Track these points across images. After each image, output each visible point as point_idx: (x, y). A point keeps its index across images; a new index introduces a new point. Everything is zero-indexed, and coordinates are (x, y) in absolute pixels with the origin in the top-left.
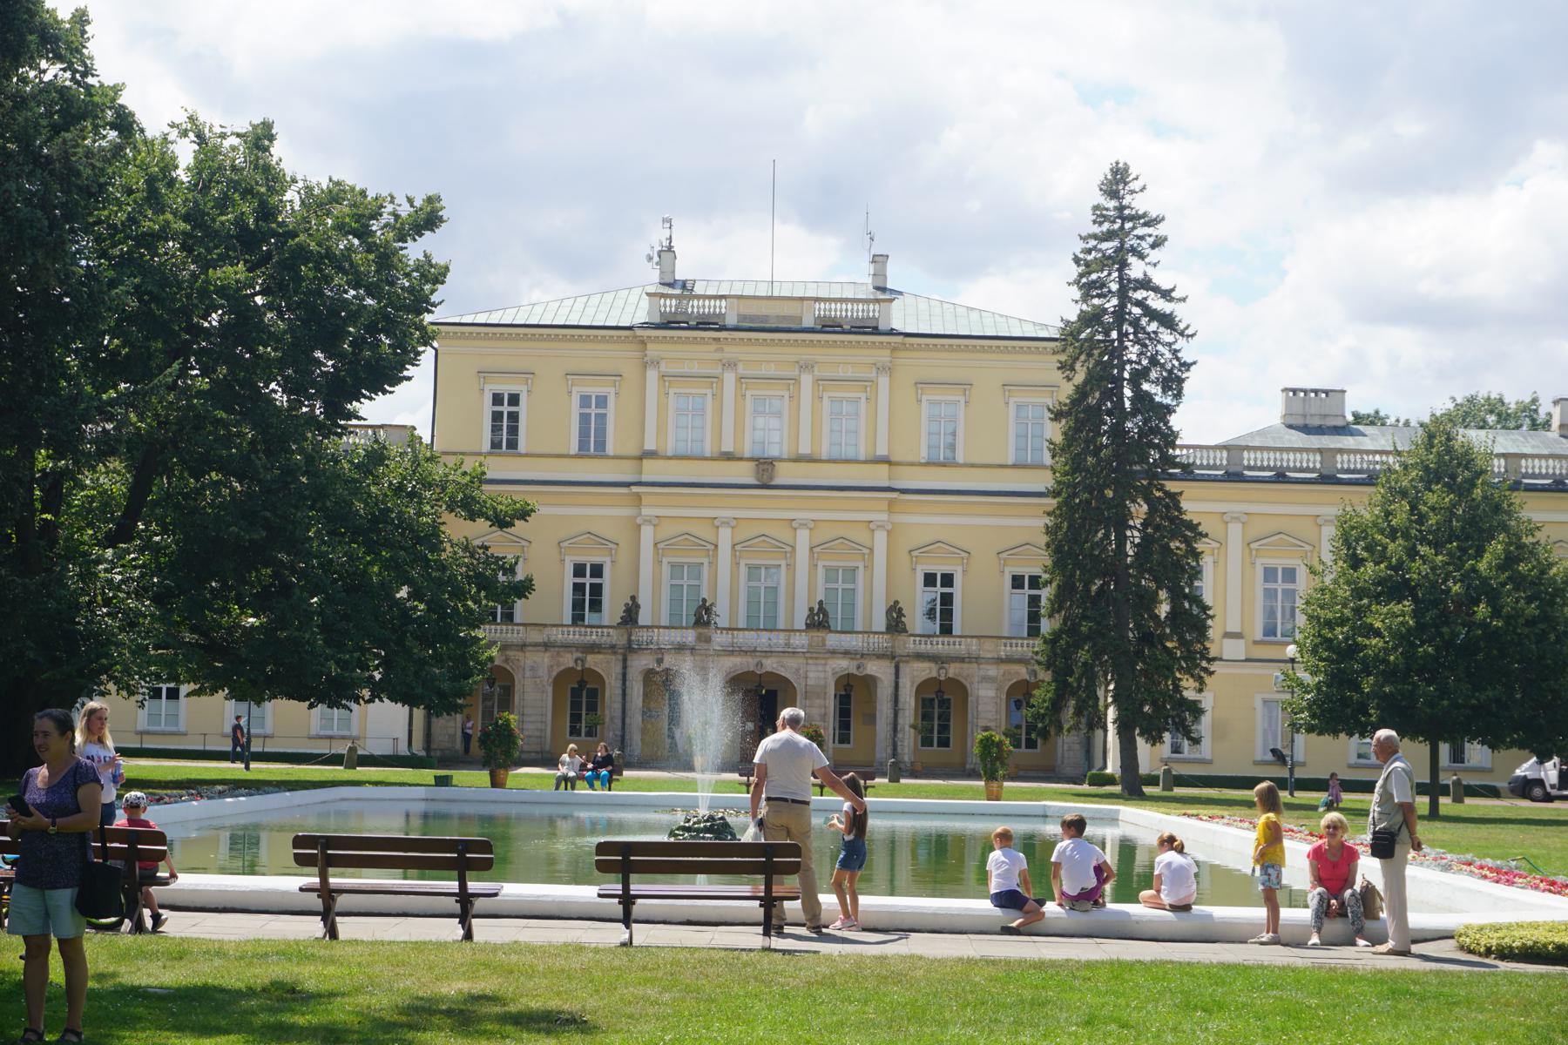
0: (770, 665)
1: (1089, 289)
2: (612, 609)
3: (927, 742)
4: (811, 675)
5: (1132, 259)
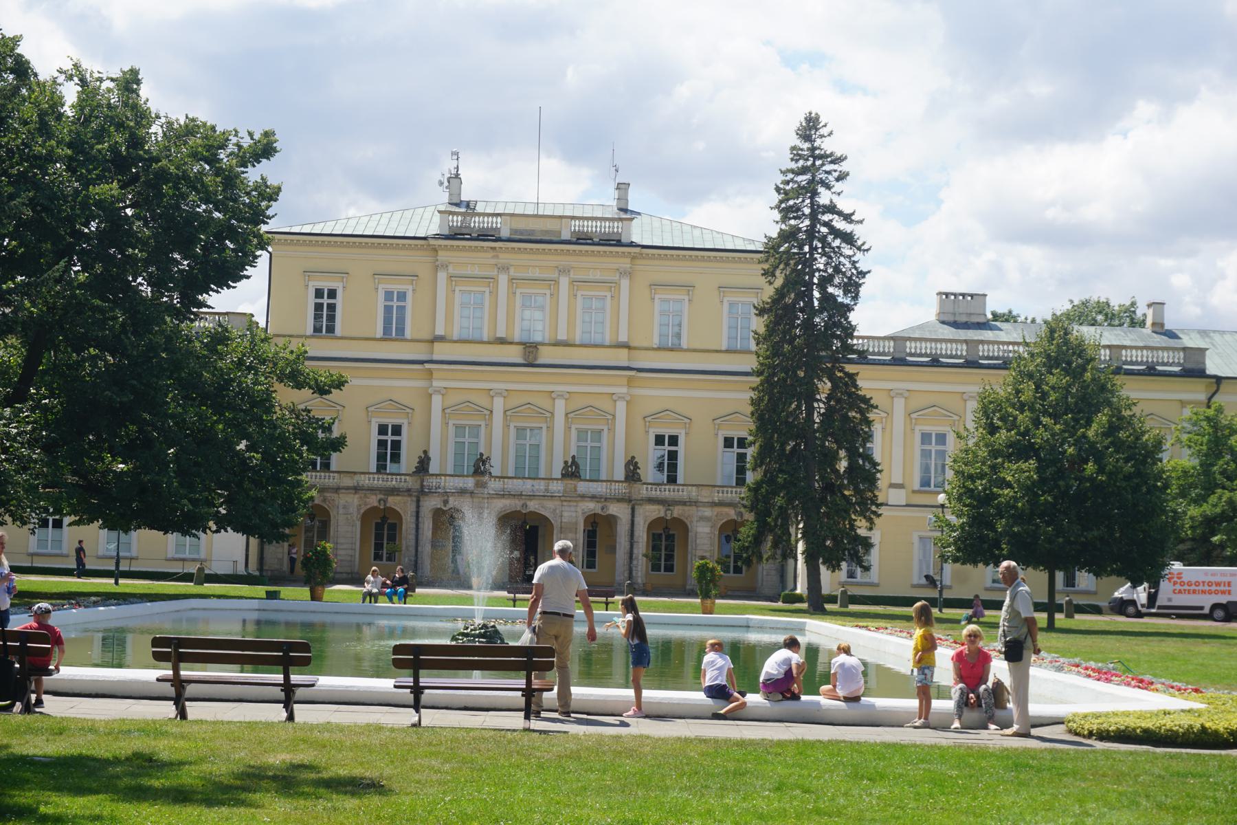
0: (533, 506)
1: (787, 212)
2: (408, 461)
3: (656, 568)
4: (565, 514)
5: (821, 189)
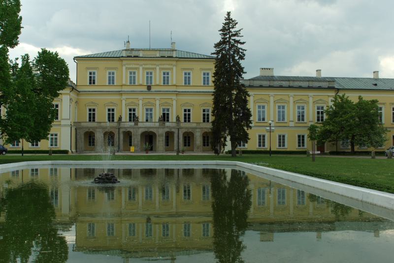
3: (185, 145)
